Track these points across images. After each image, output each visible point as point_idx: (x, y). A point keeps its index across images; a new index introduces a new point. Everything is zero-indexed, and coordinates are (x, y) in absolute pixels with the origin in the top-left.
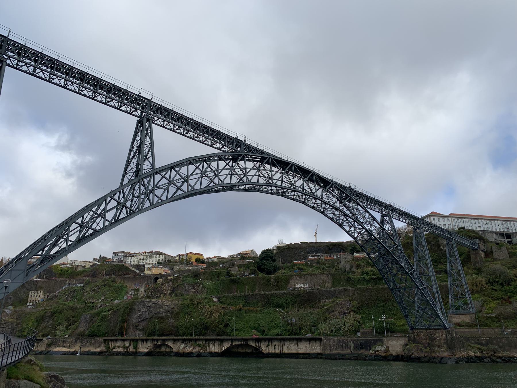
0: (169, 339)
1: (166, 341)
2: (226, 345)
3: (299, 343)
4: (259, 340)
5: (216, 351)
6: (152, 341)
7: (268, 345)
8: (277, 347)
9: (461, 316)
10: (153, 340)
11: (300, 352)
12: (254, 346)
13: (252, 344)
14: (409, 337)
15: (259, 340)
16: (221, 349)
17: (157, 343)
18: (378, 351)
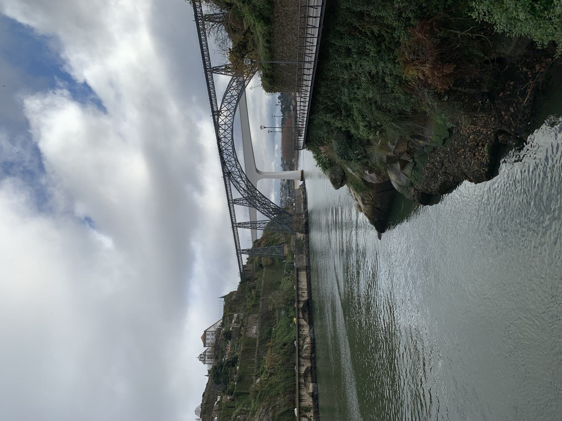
0: (299, 370)
1: (301, 374)
2: (303, 322)
3: (300, 281)
4: (299, 302)
5: (308, 330)
6: (301, 388)
7: (303, 296)
8: (303, 292)
9: (285, 250)
10: (300, 388)
11: (306, 280)
12: (303, 304)
13: (301, 305)
14: (296, 231)
15: (299, 302)
16: (307, 326)
17: (303, 383)
18: (303, 238)
